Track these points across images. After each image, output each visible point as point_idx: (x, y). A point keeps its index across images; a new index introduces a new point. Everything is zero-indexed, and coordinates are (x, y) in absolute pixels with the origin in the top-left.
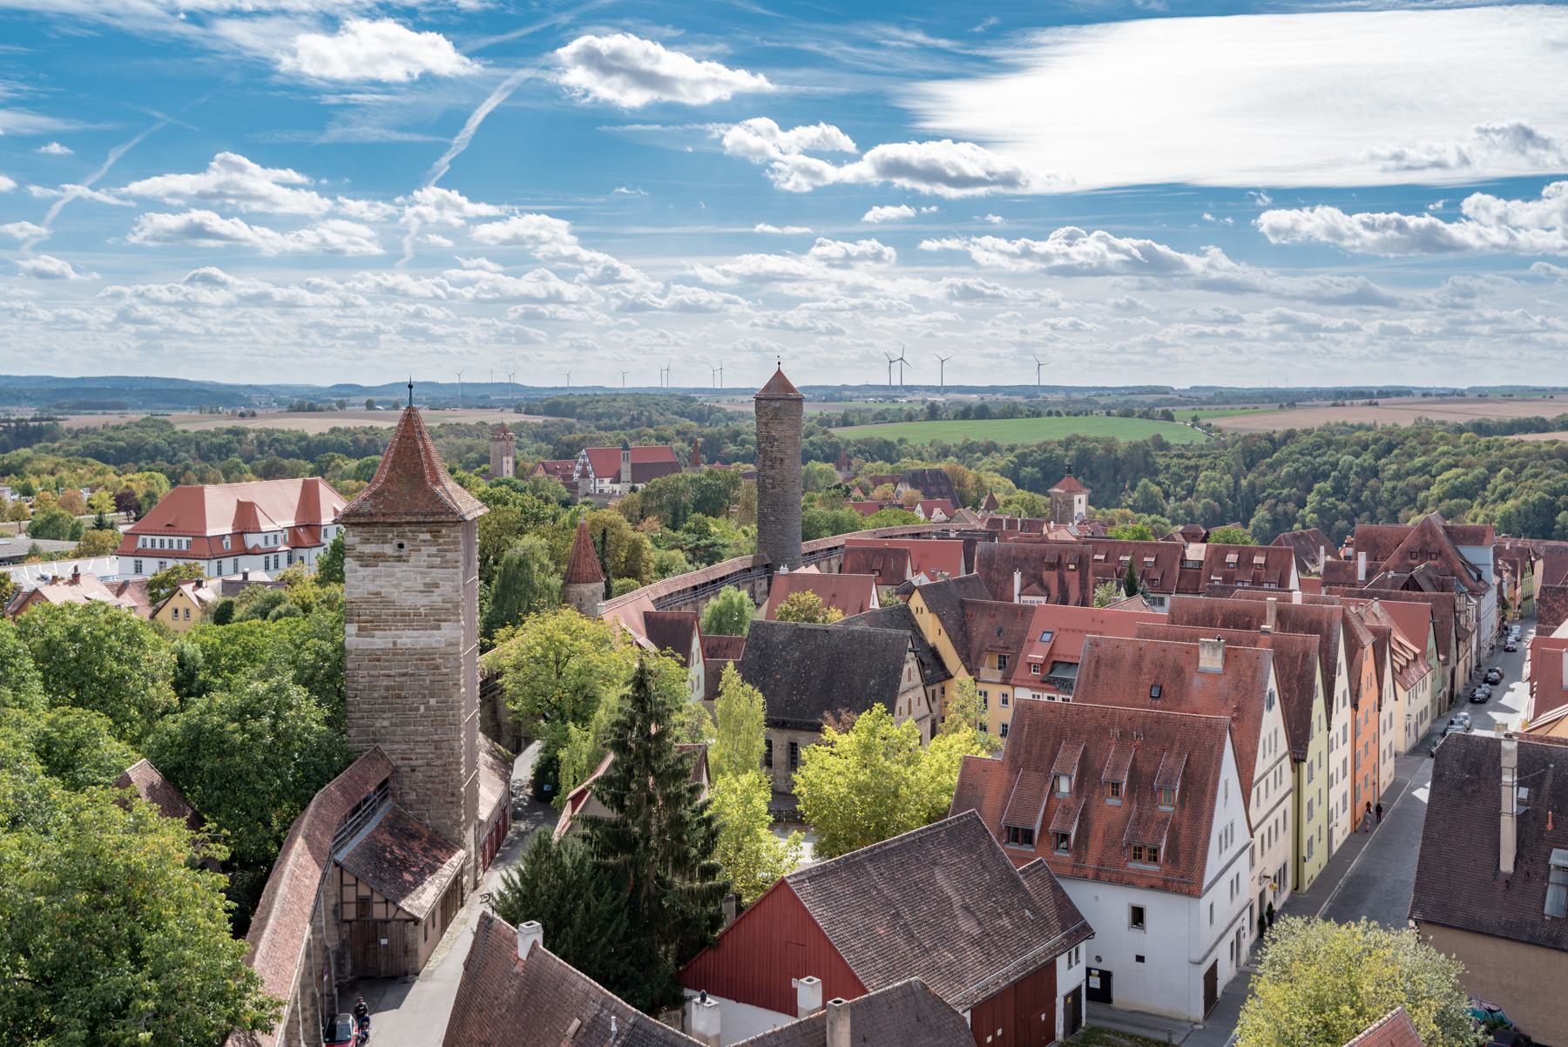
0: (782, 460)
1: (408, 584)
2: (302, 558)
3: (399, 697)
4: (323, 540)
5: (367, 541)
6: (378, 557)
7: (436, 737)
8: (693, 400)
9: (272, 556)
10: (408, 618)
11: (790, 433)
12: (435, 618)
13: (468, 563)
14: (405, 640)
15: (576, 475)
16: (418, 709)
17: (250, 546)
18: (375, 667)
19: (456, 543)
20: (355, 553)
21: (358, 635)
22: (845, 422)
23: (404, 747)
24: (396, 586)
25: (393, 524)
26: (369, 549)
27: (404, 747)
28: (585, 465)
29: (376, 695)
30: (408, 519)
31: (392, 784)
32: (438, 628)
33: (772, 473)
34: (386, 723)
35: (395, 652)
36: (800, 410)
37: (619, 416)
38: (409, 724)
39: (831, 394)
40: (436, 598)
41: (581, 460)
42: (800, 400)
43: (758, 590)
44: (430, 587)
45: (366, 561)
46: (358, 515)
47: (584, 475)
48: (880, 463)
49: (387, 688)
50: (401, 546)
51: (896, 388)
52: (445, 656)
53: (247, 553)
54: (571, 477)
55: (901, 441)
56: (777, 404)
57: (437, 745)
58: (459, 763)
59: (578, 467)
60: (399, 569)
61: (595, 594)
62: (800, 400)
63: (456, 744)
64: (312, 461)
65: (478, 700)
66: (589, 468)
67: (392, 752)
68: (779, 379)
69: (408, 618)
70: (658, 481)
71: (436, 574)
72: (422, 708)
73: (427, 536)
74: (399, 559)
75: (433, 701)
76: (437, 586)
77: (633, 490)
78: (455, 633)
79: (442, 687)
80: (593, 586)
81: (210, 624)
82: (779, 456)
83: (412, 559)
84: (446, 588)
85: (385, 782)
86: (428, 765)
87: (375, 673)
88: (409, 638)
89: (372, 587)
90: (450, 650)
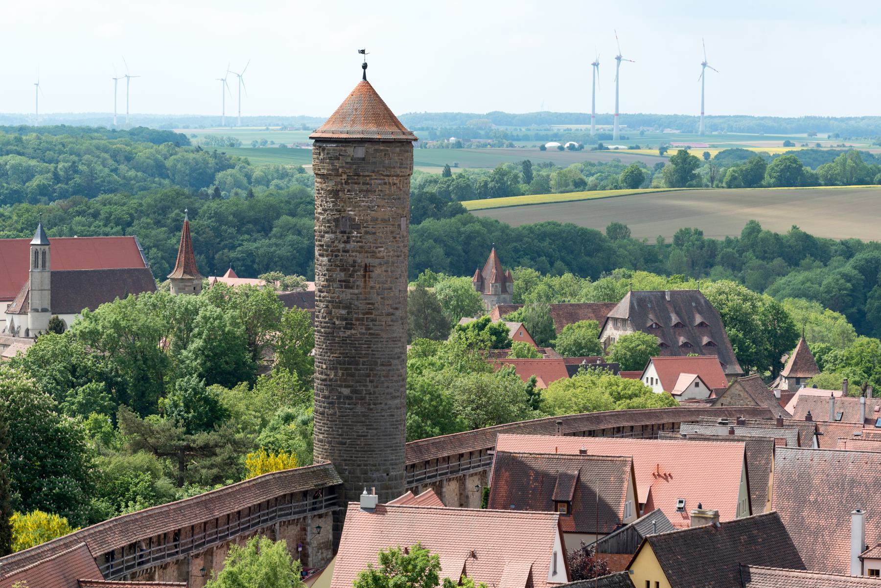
0: (367, 268)
8: (180, 141)
11: (386, 212)
22: (501, 187)
33: (346, 295)
36: (407, 165)
37: (29, 174)
39: (465, 134)
42: (405, 144)
43: (314, 540)
48: (568, 276)
51: (606, 119)
55: (617, 231)
56: (360, 152)
62: (405, 144)
68: (370, 101)
70: (107, 312)
77: (58, 327)
82: (361, 259)
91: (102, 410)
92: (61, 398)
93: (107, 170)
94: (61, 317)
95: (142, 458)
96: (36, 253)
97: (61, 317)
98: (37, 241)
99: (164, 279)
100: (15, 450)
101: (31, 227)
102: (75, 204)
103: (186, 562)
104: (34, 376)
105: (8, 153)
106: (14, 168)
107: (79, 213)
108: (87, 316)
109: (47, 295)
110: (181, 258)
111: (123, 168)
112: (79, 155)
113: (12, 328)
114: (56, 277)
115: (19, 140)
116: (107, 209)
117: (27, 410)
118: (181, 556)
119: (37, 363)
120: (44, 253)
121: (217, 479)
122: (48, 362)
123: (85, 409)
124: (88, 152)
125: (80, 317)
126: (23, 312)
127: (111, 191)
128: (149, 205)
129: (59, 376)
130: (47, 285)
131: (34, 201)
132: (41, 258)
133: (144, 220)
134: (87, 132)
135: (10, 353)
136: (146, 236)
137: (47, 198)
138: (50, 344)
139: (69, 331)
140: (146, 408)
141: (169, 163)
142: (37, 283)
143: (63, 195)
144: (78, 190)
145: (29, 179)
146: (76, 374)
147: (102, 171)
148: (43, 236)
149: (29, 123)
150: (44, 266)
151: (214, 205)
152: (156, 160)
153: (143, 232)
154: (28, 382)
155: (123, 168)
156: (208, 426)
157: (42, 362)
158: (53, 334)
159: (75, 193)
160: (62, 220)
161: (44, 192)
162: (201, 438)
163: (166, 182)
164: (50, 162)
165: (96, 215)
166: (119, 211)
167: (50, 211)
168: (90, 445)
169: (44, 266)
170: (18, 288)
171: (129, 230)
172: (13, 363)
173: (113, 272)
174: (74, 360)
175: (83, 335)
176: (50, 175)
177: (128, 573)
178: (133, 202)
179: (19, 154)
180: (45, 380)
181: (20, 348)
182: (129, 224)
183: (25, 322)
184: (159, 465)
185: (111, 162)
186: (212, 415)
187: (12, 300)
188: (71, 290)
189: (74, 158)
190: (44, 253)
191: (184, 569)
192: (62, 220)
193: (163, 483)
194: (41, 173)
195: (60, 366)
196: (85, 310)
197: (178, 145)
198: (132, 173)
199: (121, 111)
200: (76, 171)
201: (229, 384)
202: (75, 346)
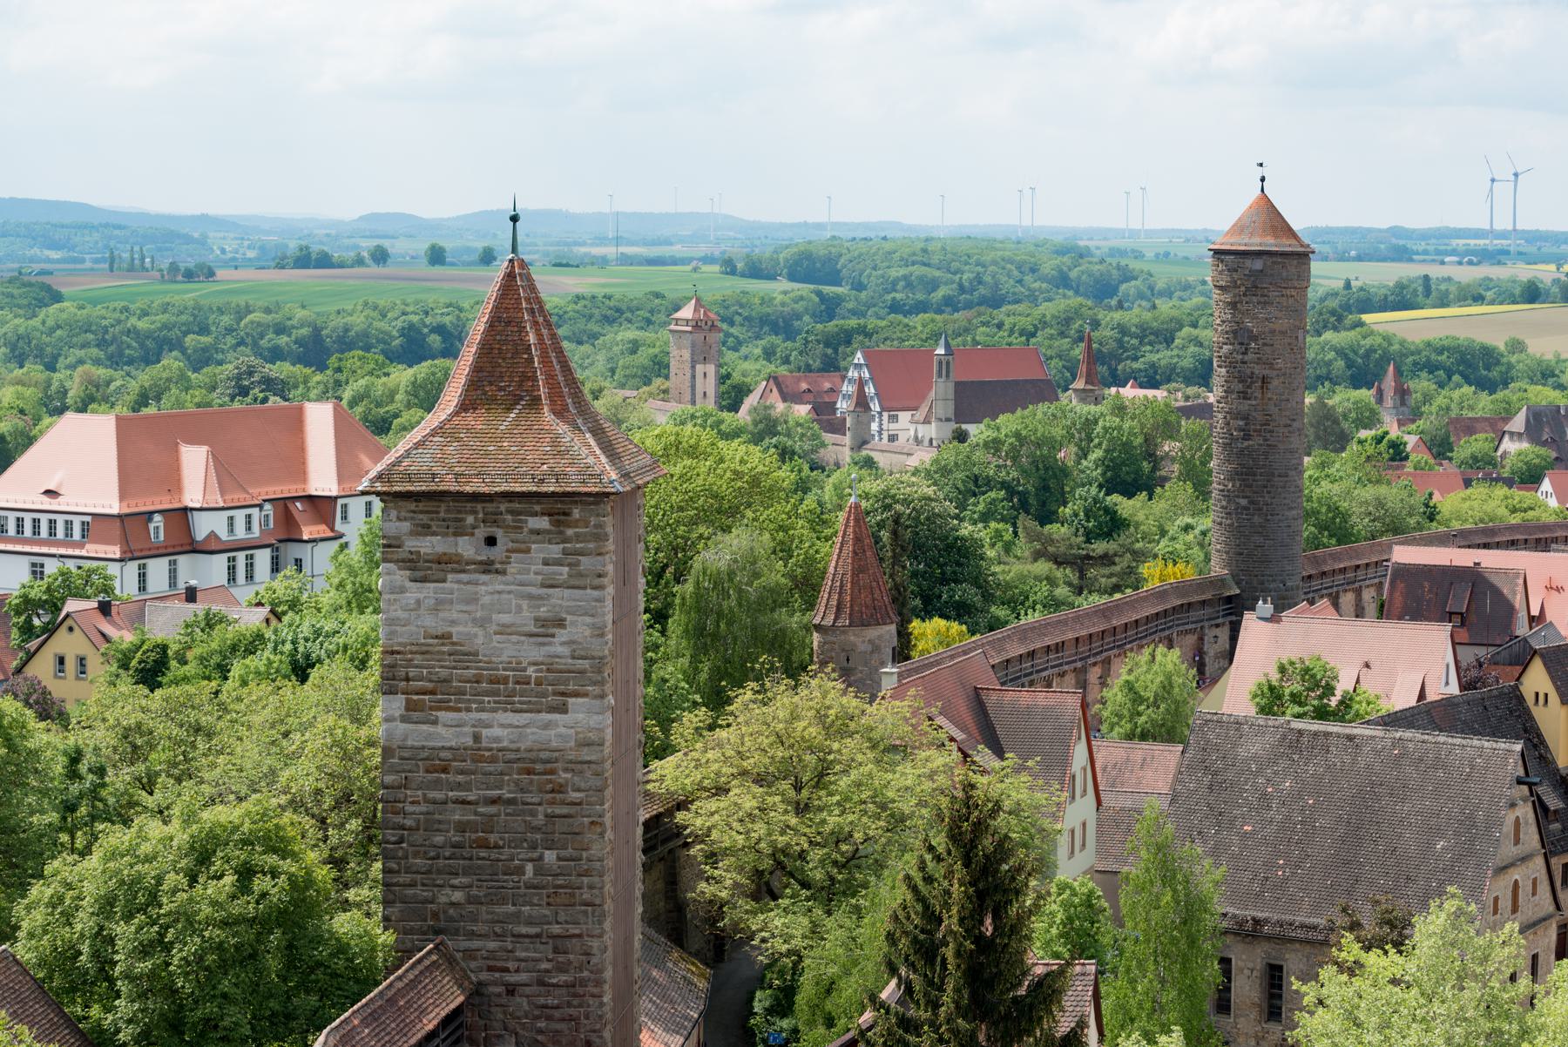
1: (506, 618)
2: (299, 563)
3: (484, 845)
4: (339, 526)
5: (424, 530)
6: (446, 564)
7: (556, 929)
9: (241, 557)
10: (505, 688)
12: (555, 690)
13: (624, 580)
14: (497, 731)
15: (842, 405)
16: (520, 871)
17: (201, 533)
18: (437, 785)
19: (600, 537)
20: (402, 554)
21: (404, 719)
23: (492, 945)
24: (482, 623)
25: (476, 497)
26: (430, 545)
27: (492, 945)
28: (861, 384)
29: (439, 839)
30: (504, 488)
31: (469, 1017)
32: (563, 709)
34: (458, 896)
35: (478, 753)
37: (934, 285)
38: (503, 901)
40: (558, 647)
41: (853, 373)
44: (550, 625)
45: (423, 569)
46: (409, 478)
47: (862, 402)
49: (462, 827)
50: (491, 541)
52: (576, 766)
53: (195, 549)
54: (831, 407)
57: (559, 943)
58: (599, 983)
59: (848, 388)
60: (488, 587)
61: (876, 649)
63: (595, 943)
64: (322, 367)
65: (640, 857)
66: (870, 390)
67: (470, 954)
69: (505, 688)
70: (1008, 423)
71: (561, 599)
72: (529, 868)
73: (543, 523)
74: (487, 567)
75: (550, 856)
76: (561, 623)
77: (961, 437)
78: (594, 720)
79: (566, 829)
80: (873, 633)
81: (126, 685)
83: (511, 569)
84: (578, 629)
85: (457, 1012)
86: (541, 983)
87: (432, 794)
88: (504, 728)
89: (430, 622)
90: (586, 754)
91: (1003, 520)
92: (962, 506)
93: (1012, 282)
94: (964, 426)
95: (1043, 567)
96: (940, 363)
97: (964, 426)
98: (941, 351)
99: (1067, 389)
100: (916, 558)
101: (935, 336)
102: (980, 315)
103: (1084, 670)
104: (935, 484)
105: (913, 264)
106: (921, 278)
107: (983, 324)
108: (989, 426)
109: (951, 406)
110: (1083, 368)
111: (1028, 278)
112: (984, 266)
113: (916, 438)
114: (960, 387)
115: (925, 251)
116: (1011, 319)
117: (928, 519)
118: (1079, 665)
119: (940, 472)
121: (1117, 588)
122: (950, 471)
123: (985, 518)
124: (994, 263)
125: (982, 426)
126: (927, 421)
127: (1018, 302)
128: (1053, 316)
129: (960, 485)
131: (939, 311)
132: (945, 368)
133: (1048, 330)
134: (991, 244)
135: (913, 462)
136: (1050, 347)
138: (951, 454)
139: (972, 440)
140: (1046, 517)
141: (1073, 274)
142: (940, 392)
143: (969, 306)
144: (983, 301)
145: (934, 289)
146: (978, 484)
147: (1008, 285)
148: (947, 346)
149: (935, 235)
151: (1117, 316)
152: (1061, 271)
153: (1047, 342)
154: (930, 491)
155: (1028, 278)
156: (1108, 535)
157: (945, 471)
158: (955, 443)
159: (980, 304)
160: (967, 330)
161: (950, 304)
162: (1100, 547)
163: (1070, 293)
164: (955, 273)
165: (1000, 326)
166: (1025, 322)
167: (955, 321)
168: (991, 553)
170: (923, 397)
171: (1033, 340)
172: (916, 472)
173: (1016, 382)
174: (976, 470)
175: (986, 444)
176: (955, 286)
177: (1026, 680)
178: (1037, 312)
179: (925, 264)
180: (947, 488)
181: (923, 457)
182: (1033, 335)
183: (931, 431)
184: (1059, 574)
185: (1016, 273)
186: (1114, 525)
187: (916, 409)
188: (973, 400)
189: (979, 269)
191: (1082, 677)
192: (967, 330)
193: (1062, 591)
194: (946, 284)
195: (960, 475)
196: (986, 420)
197: (1081, 256)
198: (1036, 285)
199: (1026, 222)
200: (980, 283)
201: (1130, 495)
202: (979, 455)
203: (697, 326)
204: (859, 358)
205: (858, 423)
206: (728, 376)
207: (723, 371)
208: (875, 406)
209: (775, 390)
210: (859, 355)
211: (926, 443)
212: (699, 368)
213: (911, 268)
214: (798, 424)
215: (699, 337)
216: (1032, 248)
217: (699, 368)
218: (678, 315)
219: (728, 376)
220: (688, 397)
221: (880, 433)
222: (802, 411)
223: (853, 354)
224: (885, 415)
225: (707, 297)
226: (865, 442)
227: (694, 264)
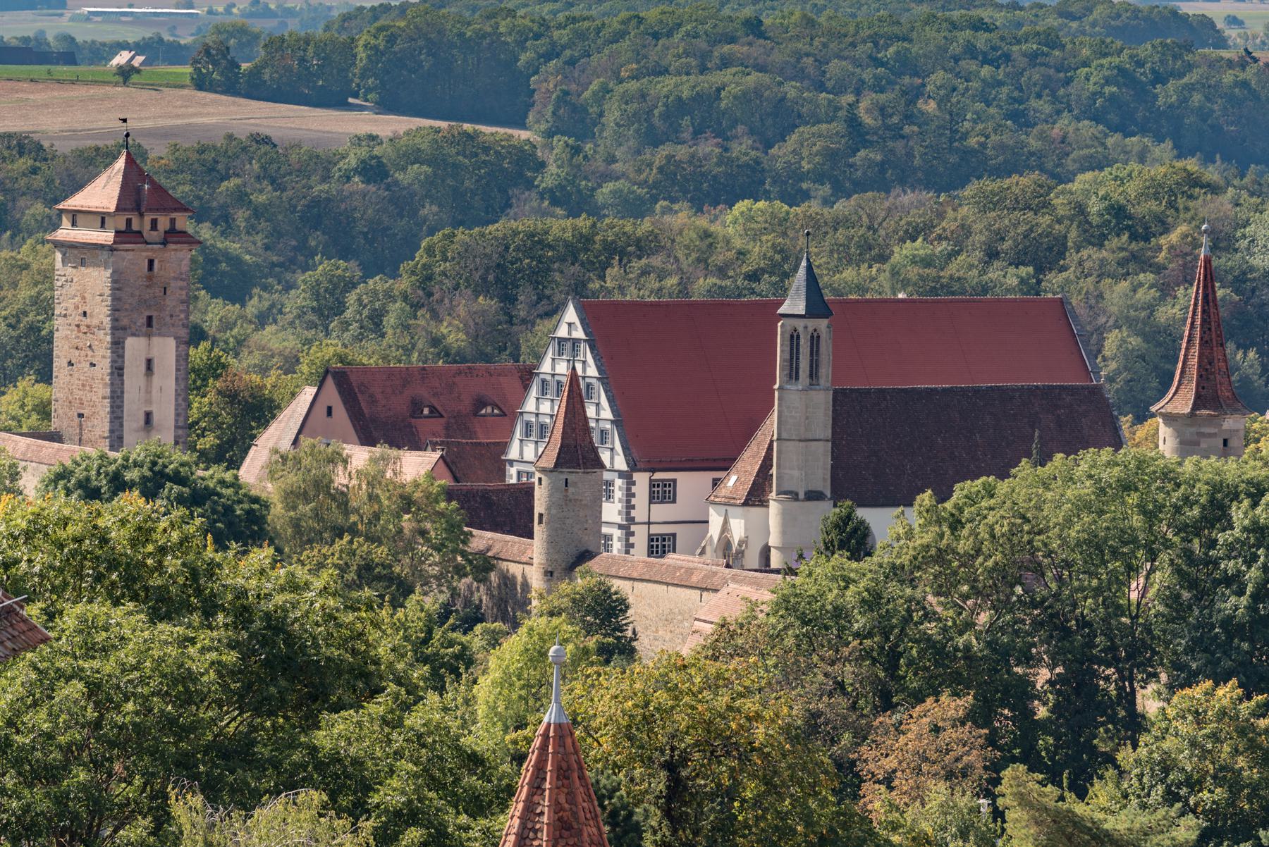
28: (576, 395)
41: (553, 366)
47: (577, 452)
66: (600, 411)
94: (862, 513)
96: (794, 338)
98: (794, 304)
99: (1142, 416)
105: (725, 63)
109: (822, 456)
110: (1190, 357)
120: (815, 340)
130: (822, 426)
137: (826, 190)
150: (814, 374)
158: (839, 559)
169: (814, 374)
176: (838, 126)
181: (745, 596)
188: (886, 447)
190: (815, 340)
196: (926, 498)
203: (126, 235)
204: (570, 323)
205: (564, 499)
206: (215, 368)
207: (198, 354)
208: (614, 457)
209: (340, 412)
210: (571, 314)
211: (752, 559)
212: (134, 346)
213: (717, 78)
214: (407, 503)
215: (135, 257)
216: (1053, 21)
217: (134, 346)
218: (78, 201)
219: (215, 368)
220: (100, 425)
221: (627, 528)
222: (415, 466)
223: (555, 311)
224: (642, 479)
225: (157, 152)
226: (585, 556)
227: (122, 58)
